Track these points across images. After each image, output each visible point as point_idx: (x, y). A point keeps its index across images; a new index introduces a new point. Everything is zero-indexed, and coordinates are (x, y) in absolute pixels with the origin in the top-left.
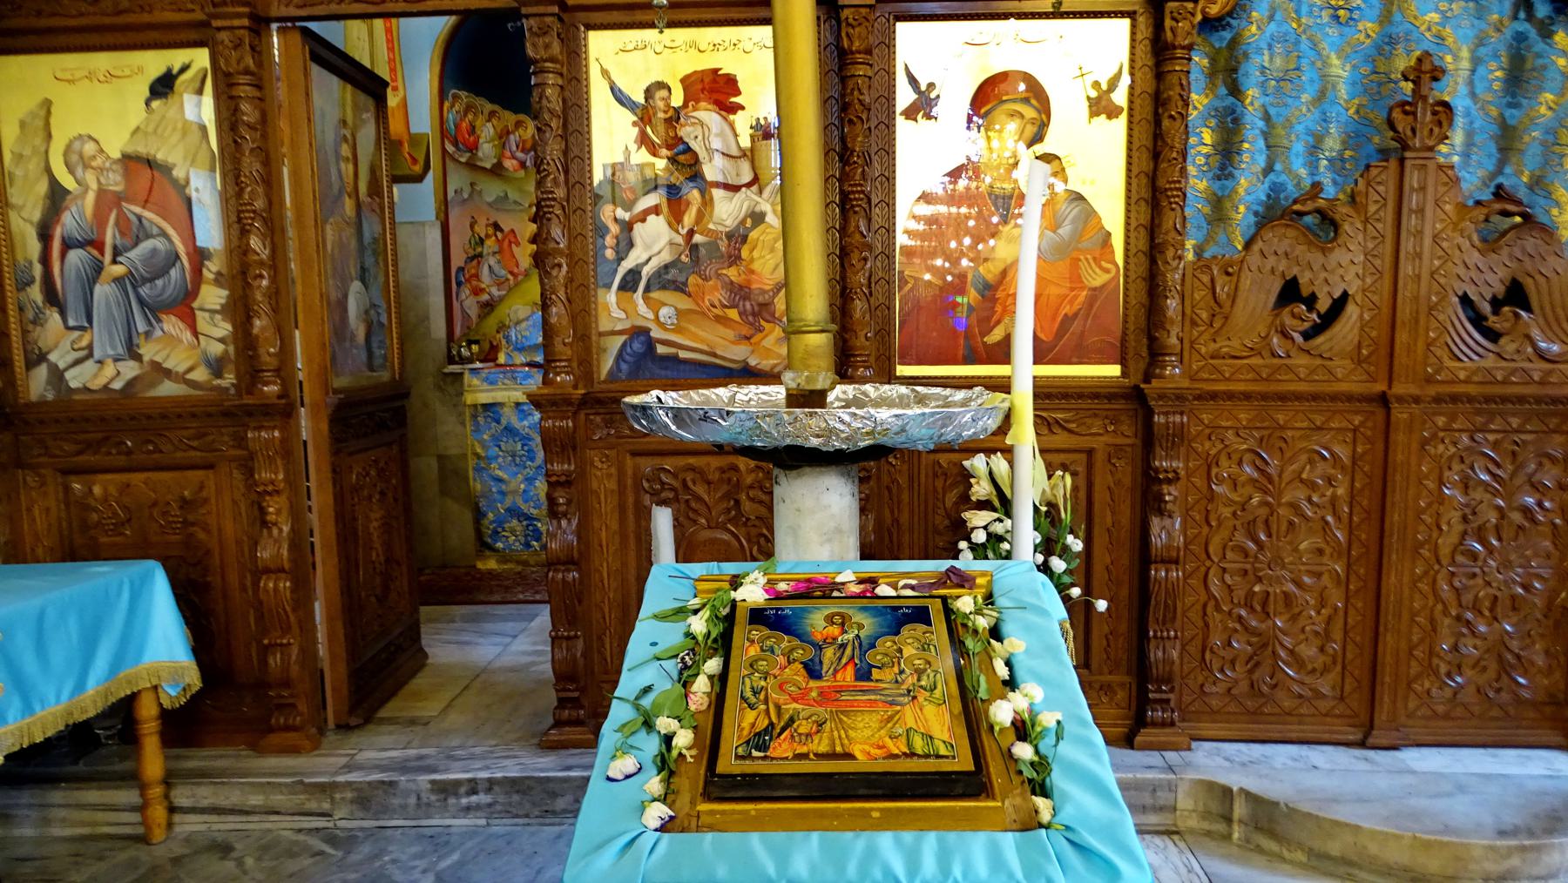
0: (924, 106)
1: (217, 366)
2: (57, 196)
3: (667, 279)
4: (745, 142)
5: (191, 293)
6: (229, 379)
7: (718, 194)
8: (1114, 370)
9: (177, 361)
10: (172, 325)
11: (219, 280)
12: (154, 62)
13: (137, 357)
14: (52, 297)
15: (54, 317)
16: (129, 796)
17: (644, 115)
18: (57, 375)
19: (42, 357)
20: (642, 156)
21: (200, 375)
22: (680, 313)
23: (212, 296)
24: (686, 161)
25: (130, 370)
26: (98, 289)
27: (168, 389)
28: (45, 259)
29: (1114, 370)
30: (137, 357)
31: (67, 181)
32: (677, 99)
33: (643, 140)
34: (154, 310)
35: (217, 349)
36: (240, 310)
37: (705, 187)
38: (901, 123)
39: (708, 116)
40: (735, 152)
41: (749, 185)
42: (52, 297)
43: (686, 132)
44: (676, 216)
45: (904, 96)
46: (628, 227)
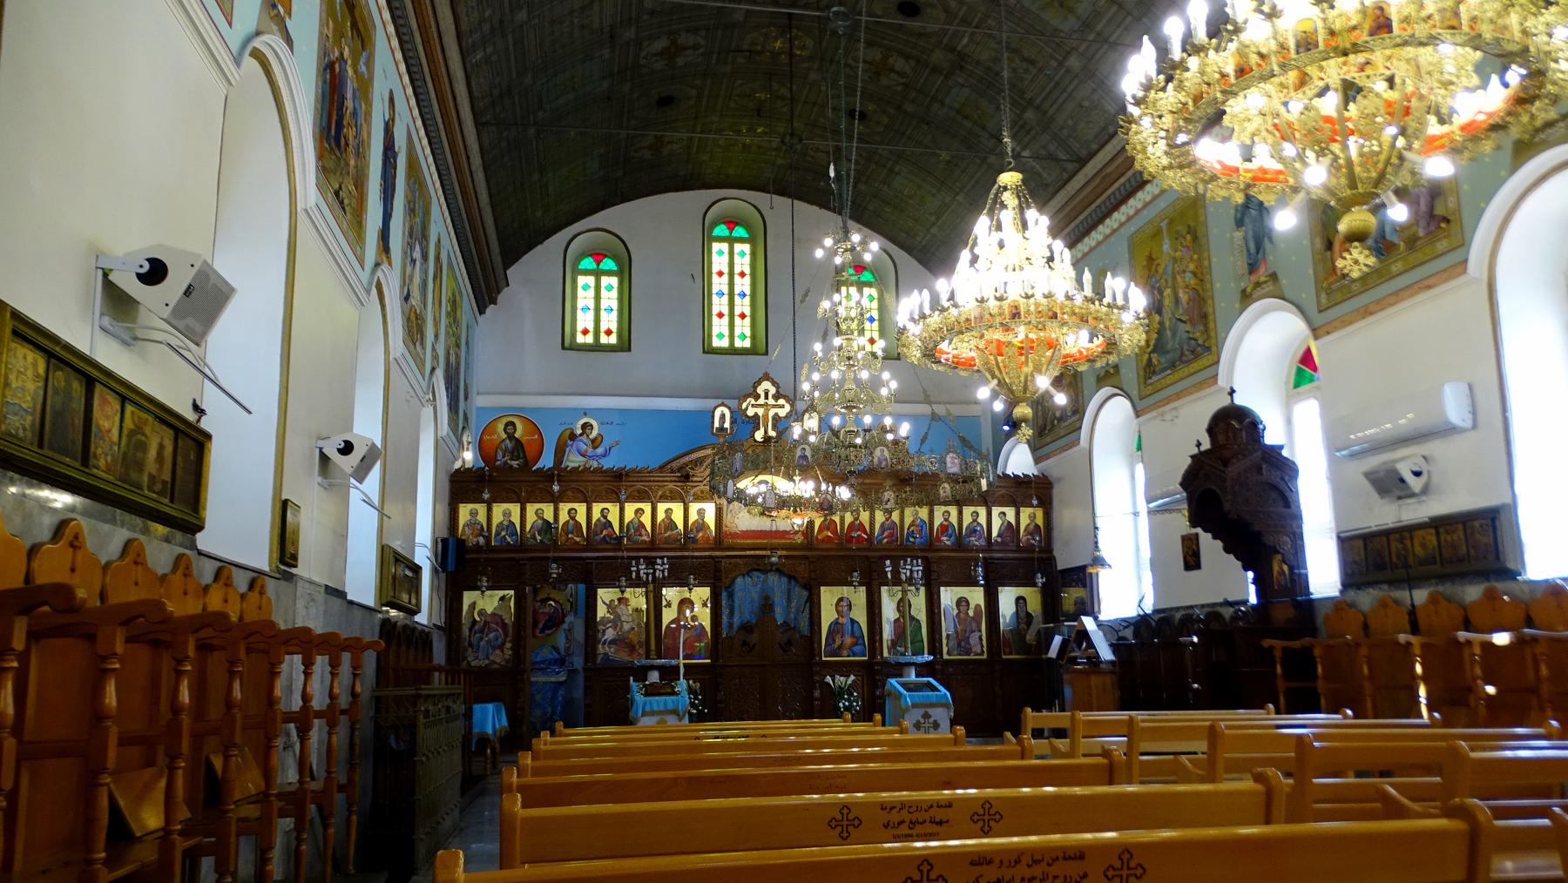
0: (669, 605)
1: (507, 661)
3: (613, 642)
5: (503, 643)
6: (510, 665)
9: (498, 660)
10: (498, 652)
11: (510, 642)
12: (501, 593)
13: (488, 658)
14: (470, 644)
15: (470, 649)
16: (483, 759)
17: (610, 606)
18: (469, 663)
19: (465, 658)
20: (608, 615)
21: (503, 663)
22: (616, 650)
23: (509, 645)
24: (618, 617)
25: (487, 662)
26: (482, 643)
27: (496, 666)
28: (470, 636)
30: (488, 658)
31: (478, 619)
32: (616, 603)
33: (608, 612)
34: (494, 648)
35: (508, 657)
37: (622, 622)
43: (618, 610)
44: (615, 629)
45: (664, 603)
46: (604, 631)
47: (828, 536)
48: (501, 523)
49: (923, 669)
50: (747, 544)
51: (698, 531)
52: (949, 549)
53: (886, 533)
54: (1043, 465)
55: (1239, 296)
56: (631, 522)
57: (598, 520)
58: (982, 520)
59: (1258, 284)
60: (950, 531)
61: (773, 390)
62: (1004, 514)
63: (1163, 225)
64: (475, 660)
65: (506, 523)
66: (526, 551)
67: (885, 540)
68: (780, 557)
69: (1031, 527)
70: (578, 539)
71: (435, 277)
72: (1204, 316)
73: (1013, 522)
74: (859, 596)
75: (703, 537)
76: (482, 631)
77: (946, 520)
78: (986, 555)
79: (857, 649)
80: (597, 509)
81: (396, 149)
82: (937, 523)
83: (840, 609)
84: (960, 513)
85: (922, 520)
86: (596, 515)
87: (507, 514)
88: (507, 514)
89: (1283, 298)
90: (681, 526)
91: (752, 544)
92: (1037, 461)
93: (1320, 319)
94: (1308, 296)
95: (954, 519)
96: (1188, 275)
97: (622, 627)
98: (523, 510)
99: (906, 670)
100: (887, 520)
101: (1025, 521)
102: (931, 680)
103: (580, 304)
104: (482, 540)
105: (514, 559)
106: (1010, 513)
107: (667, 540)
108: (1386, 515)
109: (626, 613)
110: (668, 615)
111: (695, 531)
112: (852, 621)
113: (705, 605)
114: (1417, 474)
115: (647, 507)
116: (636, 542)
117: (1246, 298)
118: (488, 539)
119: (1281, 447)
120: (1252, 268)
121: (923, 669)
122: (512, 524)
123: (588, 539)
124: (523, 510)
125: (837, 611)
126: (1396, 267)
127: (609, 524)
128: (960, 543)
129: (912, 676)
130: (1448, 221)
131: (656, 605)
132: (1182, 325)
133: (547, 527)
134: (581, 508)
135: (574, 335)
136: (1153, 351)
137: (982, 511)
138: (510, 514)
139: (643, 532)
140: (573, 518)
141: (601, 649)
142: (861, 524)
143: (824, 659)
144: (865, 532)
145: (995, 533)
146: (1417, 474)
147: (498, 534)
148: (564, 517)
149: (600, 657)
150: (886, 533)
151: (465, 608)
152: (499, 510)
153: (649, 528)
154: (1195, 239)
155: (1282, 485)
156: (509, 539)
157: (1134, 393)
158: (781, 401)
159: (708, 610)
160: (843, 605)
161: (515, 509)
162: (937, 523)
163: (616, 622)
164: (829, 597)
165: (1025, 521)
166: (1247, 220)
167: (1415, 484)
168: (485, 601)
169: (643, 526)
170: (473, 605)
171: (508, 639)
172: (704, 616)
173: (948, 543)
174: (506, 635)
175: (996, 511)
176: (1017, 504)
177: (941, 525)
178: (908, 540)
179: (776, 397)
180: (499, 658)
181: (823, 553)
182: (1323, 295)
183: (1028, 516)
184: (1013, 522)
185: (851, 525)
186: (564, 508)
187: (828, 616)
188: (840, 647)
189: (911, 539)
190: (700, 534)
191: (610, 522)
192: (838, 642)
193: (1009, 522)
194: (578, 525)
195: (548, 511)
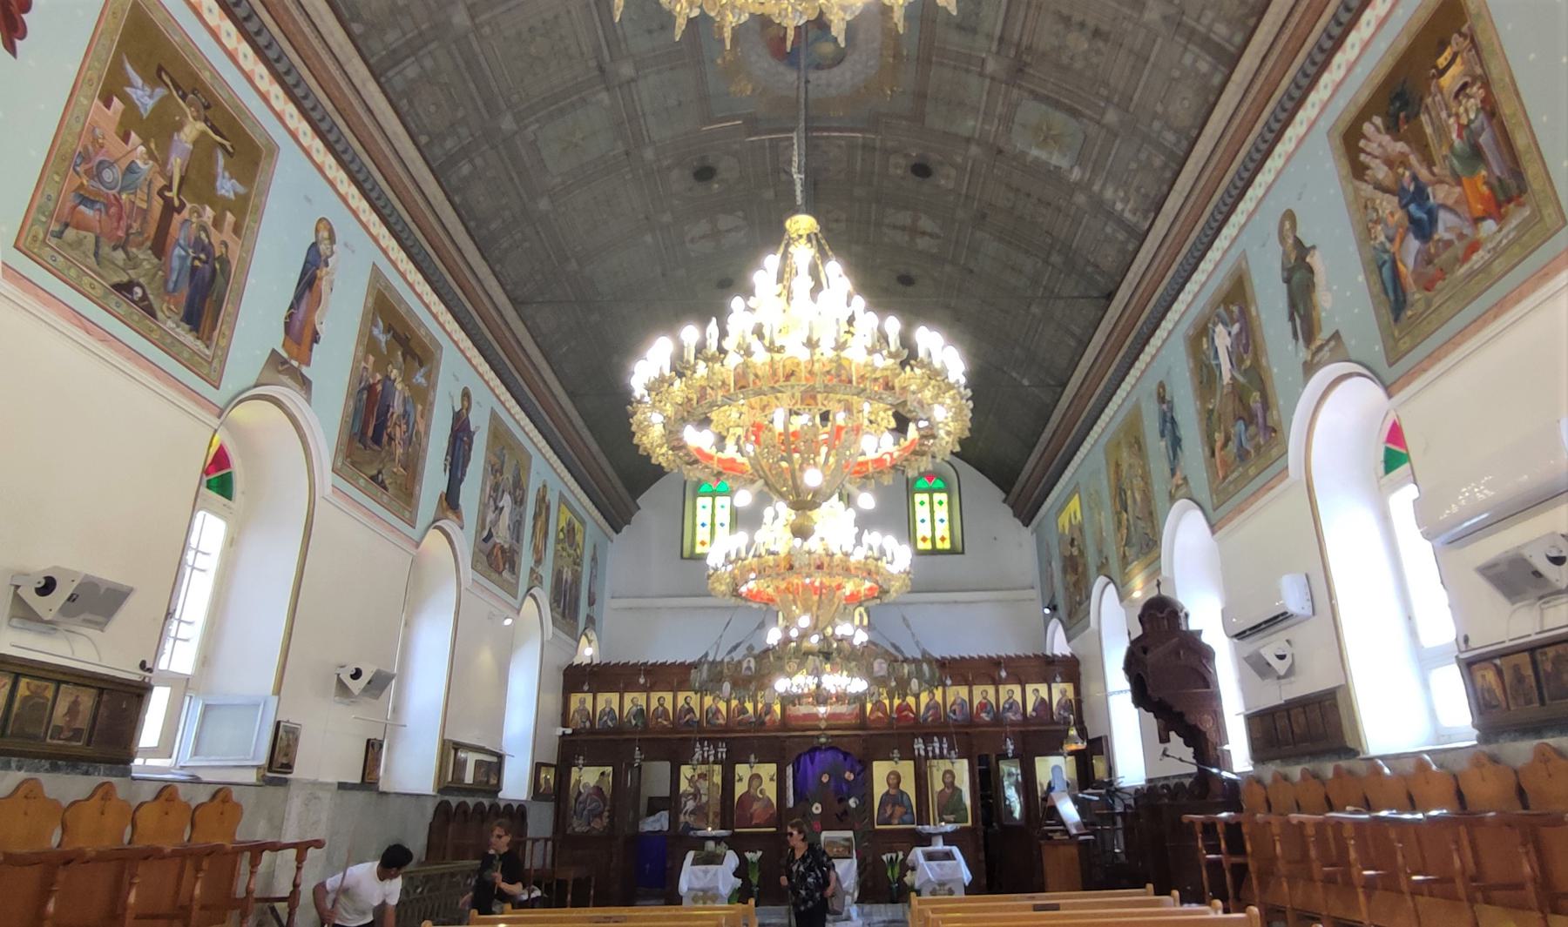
0: (740, 780)
2: (580, 793)
3: (692, 812)
8: (774, 829)
10: (598, 820)
12: (602, 769)
13: (589, 824)
14: (575, 812)
17: (690, 780)
18: (574, 829)
19: (571, 824)
23: (606, 814)
25: (588, 828)
27: (594, 833)
29: (774, 829)
34: (595, 816)
36: (611, 817)
38: (736, 783)
39: (701, 780)
42: (575, 812)
43: (698, 784)
45: (737, 778)
47: (879, 717)
48: (604, 710)
49: (948, 838)
51: (766, 715)
52: (987, 724)
54: (1074, 642)
55: (1168, 498)
57: (683, 706)
58: (1018, 697)
59: (1178, 487)
60: (989, 708)
62: (1037, 690)
63: (1122, 435)
64: (578, 826)
65: (607, 710)
66: (624, 733)
67: (930, 719)
68: (828, 737)
69: (1063, 701)
70: (665, 723)
71: (535, 517)
72: (1151, 514)
73: (1046, 697)
74: (907, 769)
76: (585, 801)
77: (985, 698)
78: (1023, 729)
79: (906, 818)
80: (681, 696)
81: (472, 429)
82: (976, 702)
84: (997, 692)
85: (963, 700)
86: (681, 702)
87: (608, 702)
88: (608, 702)
89: (1190, 499)
92: (1069, 640)
93: (1215, 517)
94: (1204, 495)
95: (992, 697)
96: (1139, 479)
97: (700, 799)
98: (621, 699)
99: (934, 839)
101: (1056, 698)
102: (955, 850)
103: (699, 521)
104: (588, 724)
105: (614, 740)
106: (1043, 689)
107: (739, 723)
108: (1274, 695)
109: (703, 785)
110: (740, 789)
112: (902, 793)
113: (772, 779)
114: (1282, 657)
116: (715, 725)
117: (1172, 499)
118: (592, 724)
119: (1200, 632)
120: (1173, 472)
121: (948, 838)
122: (612, 710)
123: (673, 723)
124: (621, 699)
126: (1252, 471)
127: (691, 710)
128: (998, 719)
129: (939, 846)
130: (1275, 431)
131: (729, 781)
132: (1139, 522)
133: (640, 713)
134: (668, 696)
135: (693, 546)
136: (1126, 545)
137: (1017, 689)
138: (611, 702)
139: (720, 716)
140: (662, 705)
141: (682, 818)
142: (908, 704)
143: (877, 827)
144: (912, 712)
145: (1030, 708)
146: (1282, 657)
147: (600, 719)
148: (654, 704)
149: (682, 826)
151: (573, 781)
152: (602, 698)
153: (724, 712)
154: (1140, 448)
155: (1202, 670)
156: (610, 723)
157: (1118, 581)
160: (894, 780)
161: (615, 697)
162: (976, 702)
163: (696, 795)
164: (881, 771)
165: (1056, 698)
166: (1166, 432)
167: (1281, 667)
168: (587, 777)
169: (718, 710)
170: (579, 781)
171: (607, 808)
172: (770, 790)
173: (987, 719)
174: (605, 806)
175: (1030, 688)
176: (1048, 680)
177: (980, 703)
180: (598, 825)
181: (875, 732)
182: (1214, 496)
183: (1060, 691)
184: (1046, 697)
186: (655, 696)
187: (880, 788)
188: (891, 816)
190: (768, 718)
192: (889, 812)
193: (1043, 699)
194: (665, 711)
195: (641, 698)
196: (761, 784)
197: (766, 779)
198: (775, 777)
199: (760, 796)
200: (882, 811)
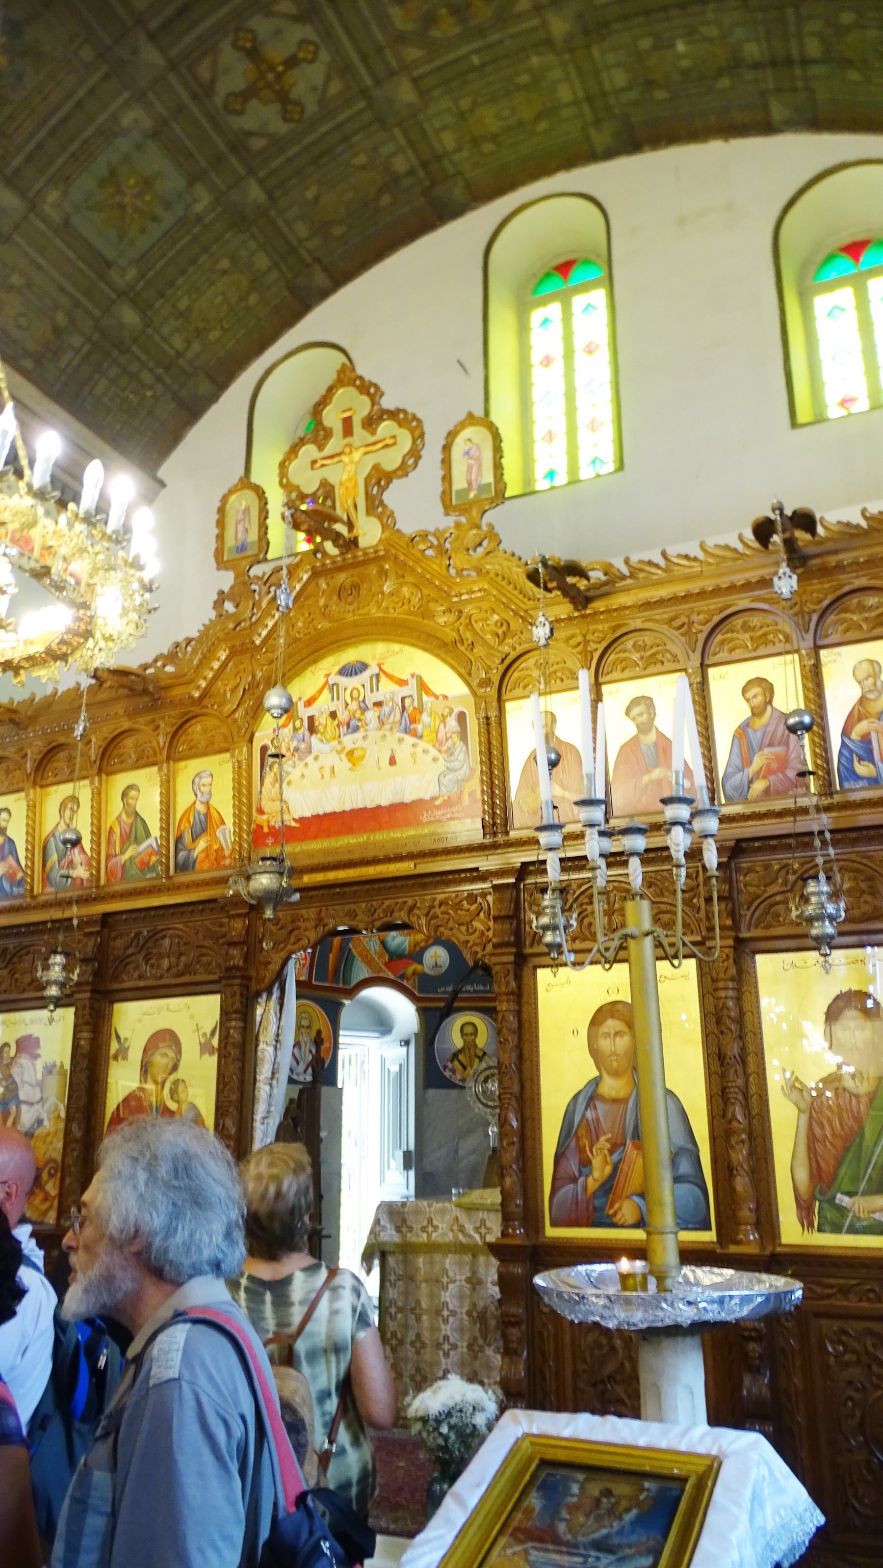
4: (39, 1076)
7: (24, 1107)
32: (13, 1052)
37: (19, 1103)
38: (113, 1063)
40: (34, 1082)
41: (38, 1102)
45: (114, 1046)
50: (311, 855)
53: (758, 762)
56: (53, 834)
61: (362, 407)
67: (759, 786)
75: (207, 850)
83: (605, 1044)
90: (155, 830)
91: (326, 852)
100: (757, 713)
111: (187, 837)
113: (206, 1048)
115: (84, 790)
125: (595, 1052)
143: (552, 1232)
150: (758, 762)
158: (386, 427)
159: (215, 1058)
178: (849, 773)
179: (370, 423)
185: (630, 748)
188: (608, 1187)
189: (863, 769)
190: (202, 844)
191: (11, 841)
192: (599, 1170)
196: (175, 1068)
197: (190, 1045)
198: (215, 1042)
199: (172, 1106)
200: (573, 1166)
